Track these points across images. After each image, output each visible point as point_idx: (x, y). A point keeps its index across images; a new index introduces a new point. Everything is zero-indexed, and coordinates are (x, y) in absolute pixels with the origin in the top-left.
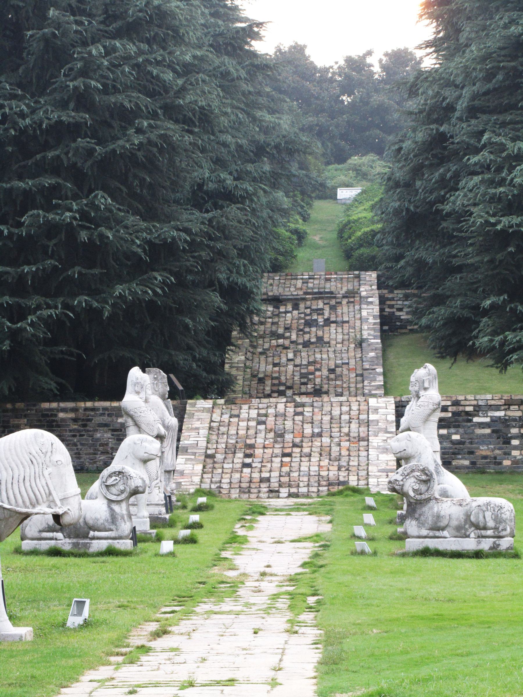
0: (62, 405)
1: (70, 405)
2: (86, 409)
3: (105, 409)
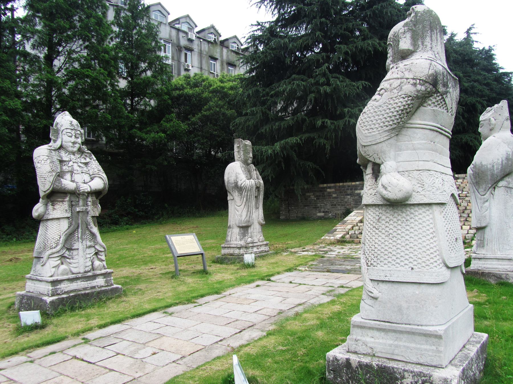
0: (329, 185)
1: (332, 185)
2: (340, 186)
3: (349, 186)
